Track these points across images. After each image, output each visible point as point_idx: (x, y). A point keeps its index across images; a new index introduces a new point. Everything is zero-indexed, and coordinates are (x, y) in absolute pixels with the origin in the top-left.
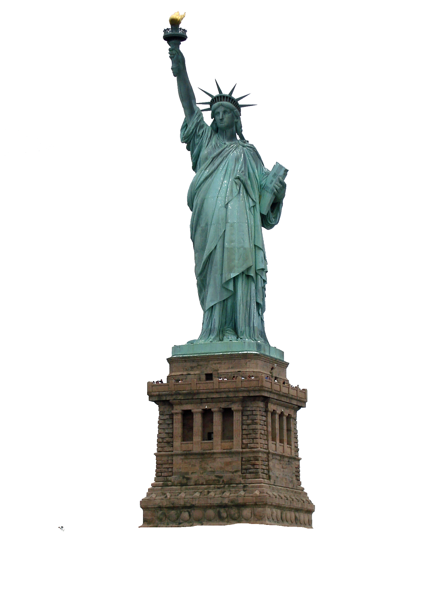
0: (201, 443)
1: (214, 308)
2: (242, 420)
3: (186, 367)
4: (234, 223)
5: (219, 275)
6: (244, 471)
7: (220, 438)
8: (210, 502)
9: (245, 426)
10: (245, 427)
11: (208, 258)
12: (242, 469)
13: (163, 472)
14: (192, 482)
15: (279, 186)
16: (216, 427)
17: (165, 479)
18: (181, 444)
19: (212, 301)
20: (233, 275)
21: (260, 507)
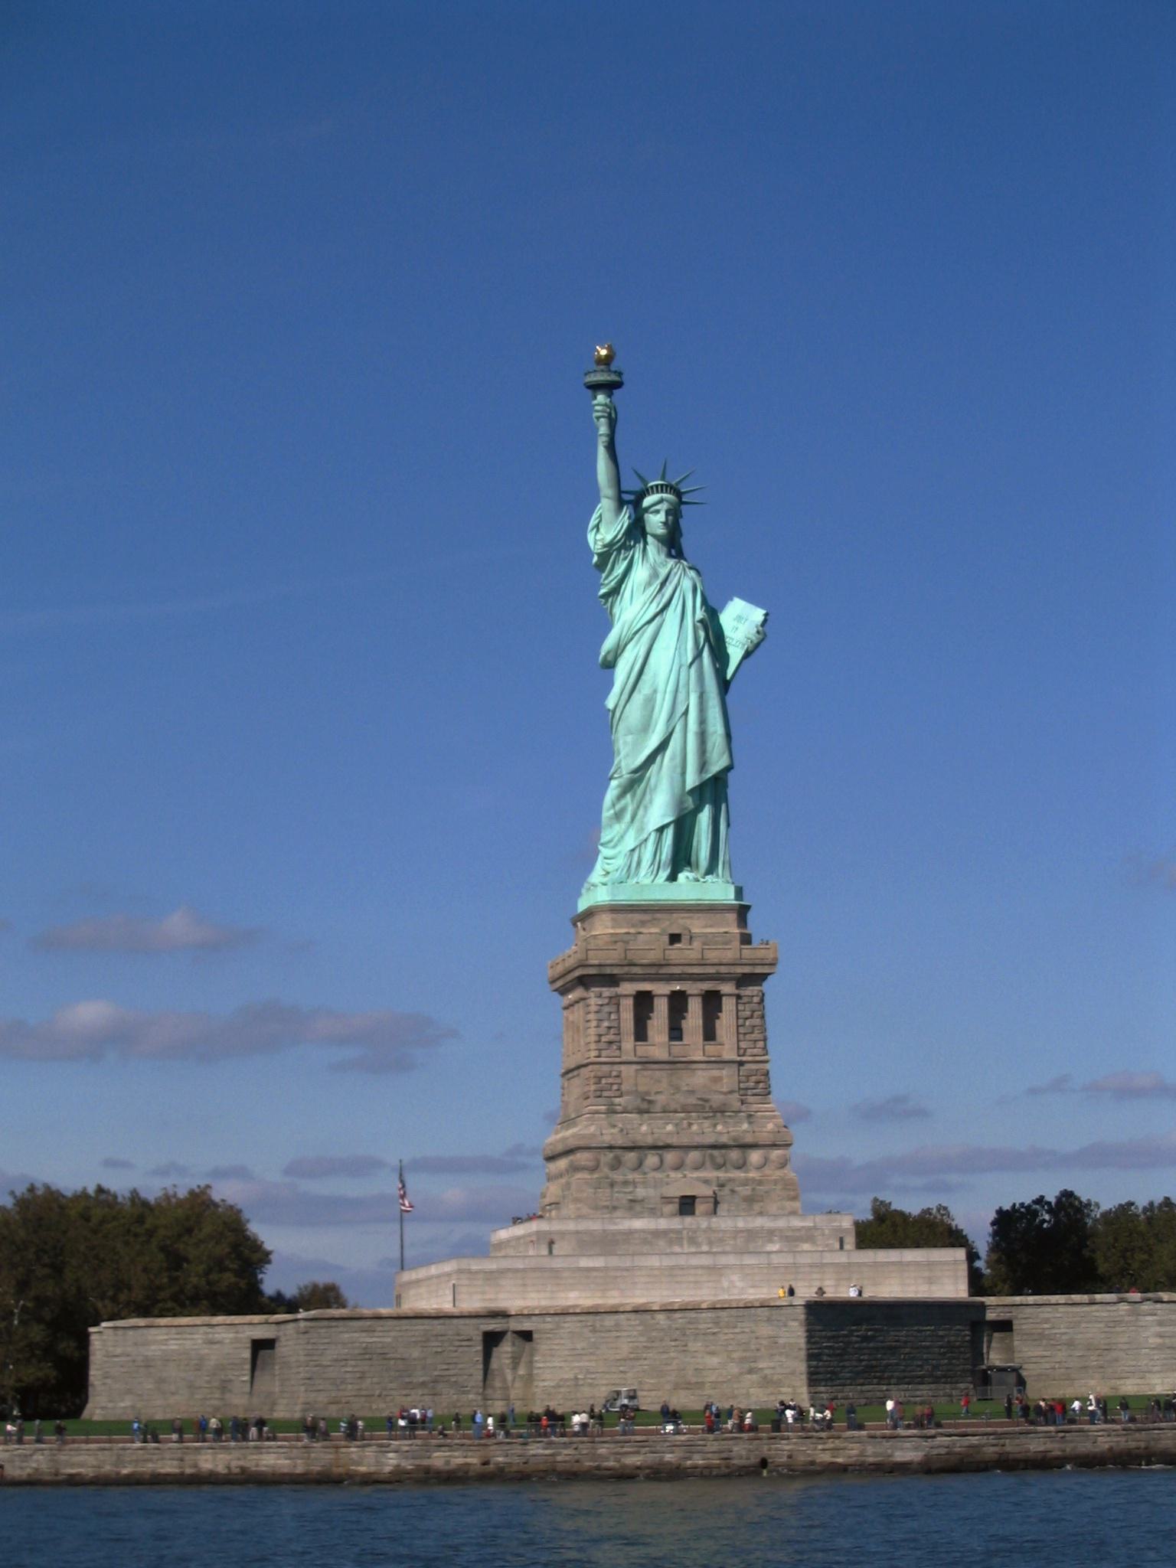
0: (670, 1046)
6: (742, 1092)
10: (741, 1022)
12: (739, 1089)
18: (635, 1046)
19: (664, 816)
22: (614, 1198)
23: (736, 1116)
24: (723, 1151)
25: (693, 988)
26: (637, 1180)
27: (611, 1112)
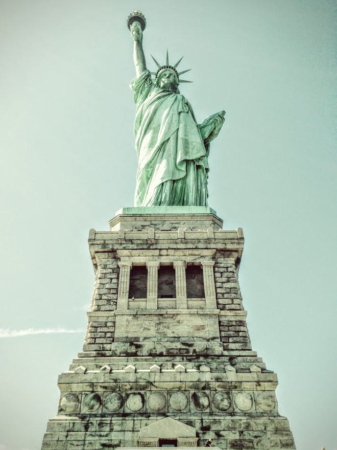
1: (165, 184)
7: (186, 296)
10: (218, 285)
12: (221, 337)
14: (145, 351)
16: (179, 281)
20: (188, 158)
24: (207, 392)
26: (114, 422)
27: (101, 354)
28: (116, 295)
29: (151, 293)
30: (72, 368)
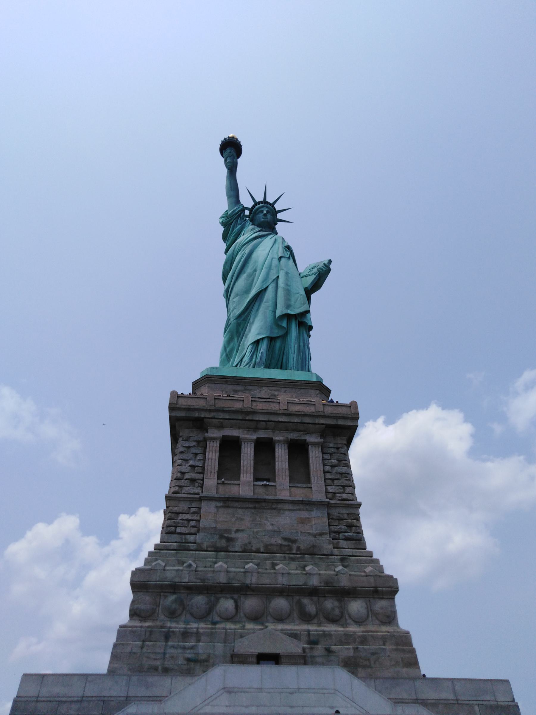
1: (261, 341)
2: (323, 459)
3: (227, 390)
4: (290, 274)
5: (271, 311)
6: (334, 534)
8: (282, 580)
9: (328, 467)
11: (255, 298)
12: (330, 532)
13: (178, 526)
15: (325, 269)
16: (280, 463)
17: (182, 539)
19: (259, 334)
21: (382, 598)
22: (167, 655)
23: (328, 559)
24: (315, 598)
25: (278, 437)
27: (183, 547)
28: (202, 475)
29: (245, 475)
30: (147, 562)
